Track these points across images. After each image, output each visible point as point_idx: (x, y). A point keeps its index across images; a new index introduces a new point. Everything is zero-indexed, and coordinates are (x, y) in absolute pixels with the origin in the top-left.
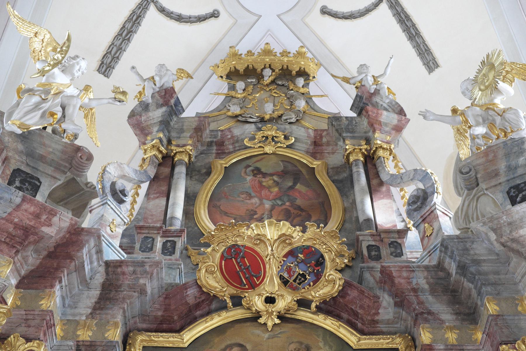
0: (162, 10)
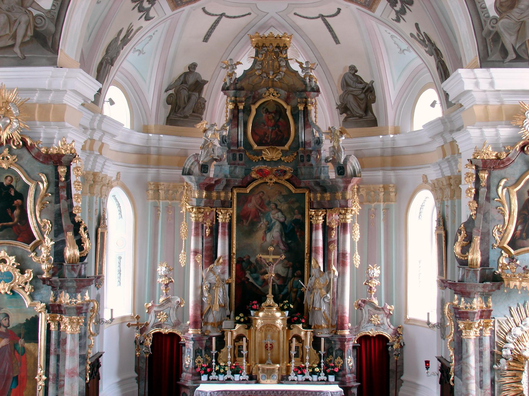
0: (228, 17)
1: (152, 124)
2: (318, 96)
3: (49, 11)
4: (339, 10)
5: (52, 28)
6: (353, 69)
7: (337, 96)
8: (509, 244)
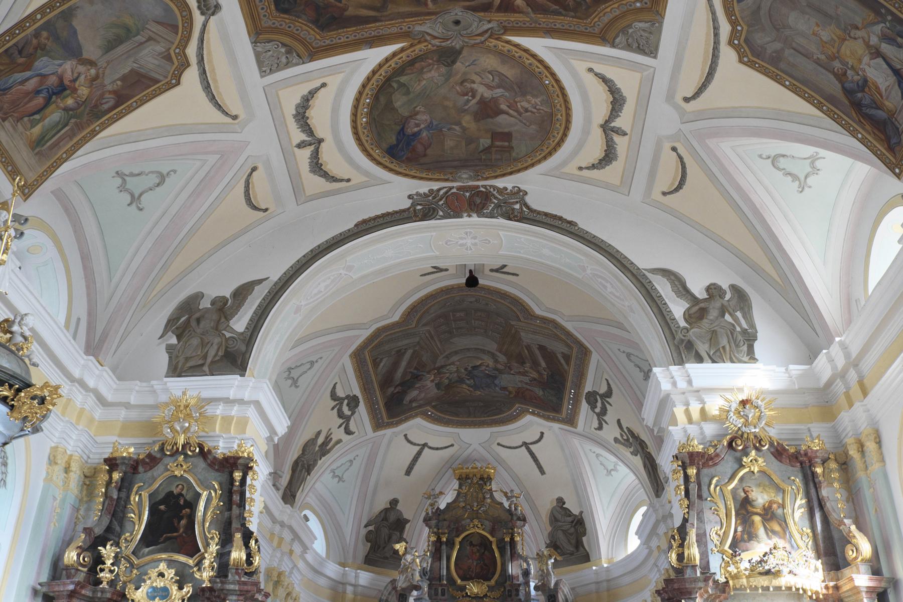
1: (350, 561)
2: (524, 525)
3: (242, 333)
4: (542, 433)
5: (243, 348)
6: (561, 501)
7: (546, 533)
8: (730, 548)
